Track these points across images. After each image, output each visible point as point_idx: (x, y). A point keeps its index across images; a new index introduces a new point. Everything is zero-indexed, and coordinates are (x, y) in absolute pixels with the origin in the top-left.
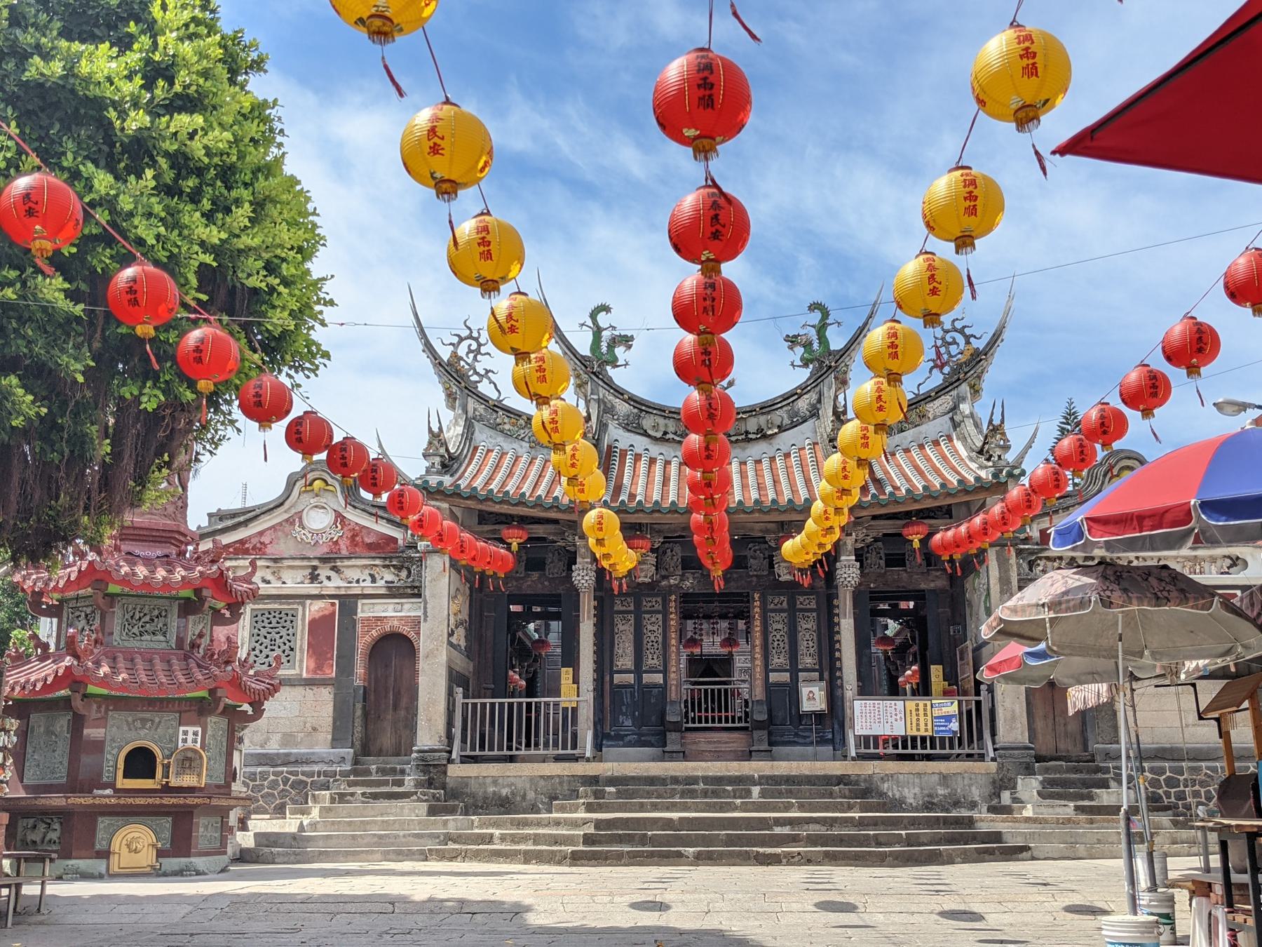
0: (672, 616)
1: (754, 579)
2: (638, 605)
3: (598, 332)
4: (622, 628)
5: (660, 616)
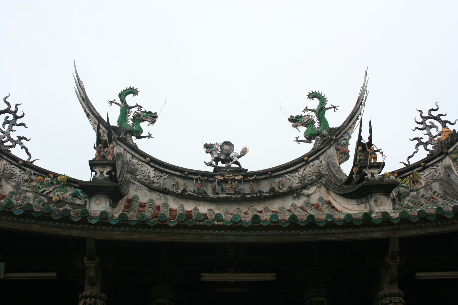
3: (125, 109)
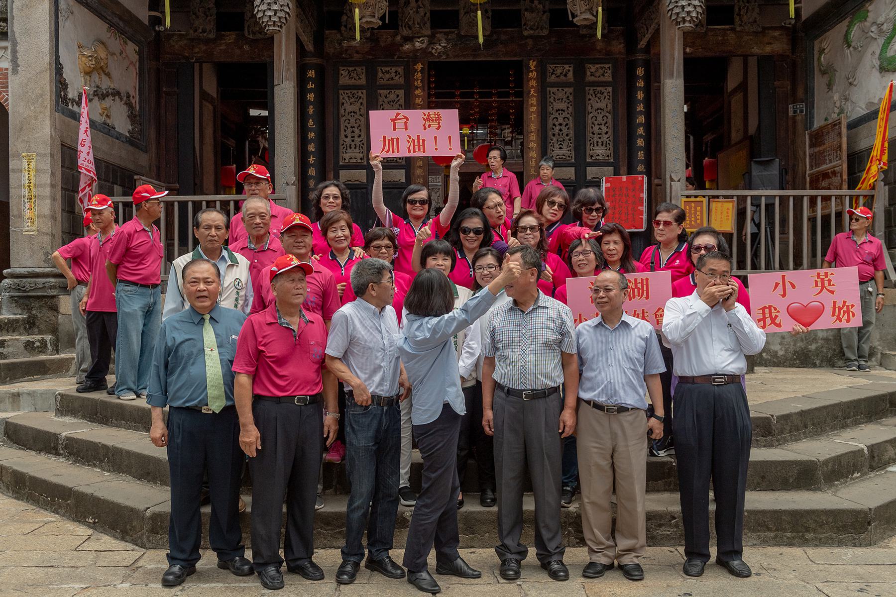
0: (418, 92)
1: (530, 42)
2: (372, 76)
4: (350, 108)
5: (401, 93)
